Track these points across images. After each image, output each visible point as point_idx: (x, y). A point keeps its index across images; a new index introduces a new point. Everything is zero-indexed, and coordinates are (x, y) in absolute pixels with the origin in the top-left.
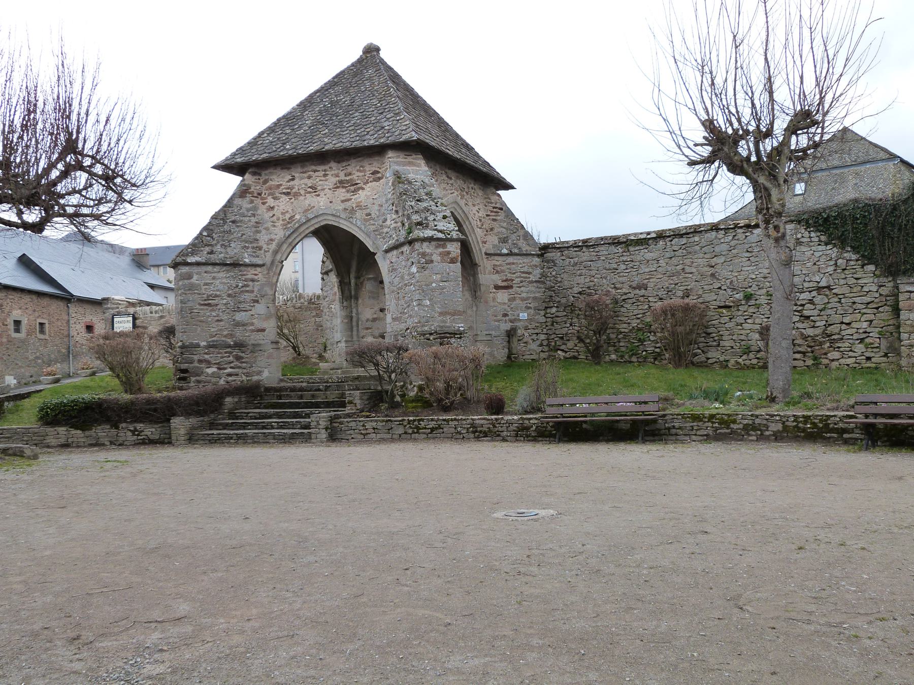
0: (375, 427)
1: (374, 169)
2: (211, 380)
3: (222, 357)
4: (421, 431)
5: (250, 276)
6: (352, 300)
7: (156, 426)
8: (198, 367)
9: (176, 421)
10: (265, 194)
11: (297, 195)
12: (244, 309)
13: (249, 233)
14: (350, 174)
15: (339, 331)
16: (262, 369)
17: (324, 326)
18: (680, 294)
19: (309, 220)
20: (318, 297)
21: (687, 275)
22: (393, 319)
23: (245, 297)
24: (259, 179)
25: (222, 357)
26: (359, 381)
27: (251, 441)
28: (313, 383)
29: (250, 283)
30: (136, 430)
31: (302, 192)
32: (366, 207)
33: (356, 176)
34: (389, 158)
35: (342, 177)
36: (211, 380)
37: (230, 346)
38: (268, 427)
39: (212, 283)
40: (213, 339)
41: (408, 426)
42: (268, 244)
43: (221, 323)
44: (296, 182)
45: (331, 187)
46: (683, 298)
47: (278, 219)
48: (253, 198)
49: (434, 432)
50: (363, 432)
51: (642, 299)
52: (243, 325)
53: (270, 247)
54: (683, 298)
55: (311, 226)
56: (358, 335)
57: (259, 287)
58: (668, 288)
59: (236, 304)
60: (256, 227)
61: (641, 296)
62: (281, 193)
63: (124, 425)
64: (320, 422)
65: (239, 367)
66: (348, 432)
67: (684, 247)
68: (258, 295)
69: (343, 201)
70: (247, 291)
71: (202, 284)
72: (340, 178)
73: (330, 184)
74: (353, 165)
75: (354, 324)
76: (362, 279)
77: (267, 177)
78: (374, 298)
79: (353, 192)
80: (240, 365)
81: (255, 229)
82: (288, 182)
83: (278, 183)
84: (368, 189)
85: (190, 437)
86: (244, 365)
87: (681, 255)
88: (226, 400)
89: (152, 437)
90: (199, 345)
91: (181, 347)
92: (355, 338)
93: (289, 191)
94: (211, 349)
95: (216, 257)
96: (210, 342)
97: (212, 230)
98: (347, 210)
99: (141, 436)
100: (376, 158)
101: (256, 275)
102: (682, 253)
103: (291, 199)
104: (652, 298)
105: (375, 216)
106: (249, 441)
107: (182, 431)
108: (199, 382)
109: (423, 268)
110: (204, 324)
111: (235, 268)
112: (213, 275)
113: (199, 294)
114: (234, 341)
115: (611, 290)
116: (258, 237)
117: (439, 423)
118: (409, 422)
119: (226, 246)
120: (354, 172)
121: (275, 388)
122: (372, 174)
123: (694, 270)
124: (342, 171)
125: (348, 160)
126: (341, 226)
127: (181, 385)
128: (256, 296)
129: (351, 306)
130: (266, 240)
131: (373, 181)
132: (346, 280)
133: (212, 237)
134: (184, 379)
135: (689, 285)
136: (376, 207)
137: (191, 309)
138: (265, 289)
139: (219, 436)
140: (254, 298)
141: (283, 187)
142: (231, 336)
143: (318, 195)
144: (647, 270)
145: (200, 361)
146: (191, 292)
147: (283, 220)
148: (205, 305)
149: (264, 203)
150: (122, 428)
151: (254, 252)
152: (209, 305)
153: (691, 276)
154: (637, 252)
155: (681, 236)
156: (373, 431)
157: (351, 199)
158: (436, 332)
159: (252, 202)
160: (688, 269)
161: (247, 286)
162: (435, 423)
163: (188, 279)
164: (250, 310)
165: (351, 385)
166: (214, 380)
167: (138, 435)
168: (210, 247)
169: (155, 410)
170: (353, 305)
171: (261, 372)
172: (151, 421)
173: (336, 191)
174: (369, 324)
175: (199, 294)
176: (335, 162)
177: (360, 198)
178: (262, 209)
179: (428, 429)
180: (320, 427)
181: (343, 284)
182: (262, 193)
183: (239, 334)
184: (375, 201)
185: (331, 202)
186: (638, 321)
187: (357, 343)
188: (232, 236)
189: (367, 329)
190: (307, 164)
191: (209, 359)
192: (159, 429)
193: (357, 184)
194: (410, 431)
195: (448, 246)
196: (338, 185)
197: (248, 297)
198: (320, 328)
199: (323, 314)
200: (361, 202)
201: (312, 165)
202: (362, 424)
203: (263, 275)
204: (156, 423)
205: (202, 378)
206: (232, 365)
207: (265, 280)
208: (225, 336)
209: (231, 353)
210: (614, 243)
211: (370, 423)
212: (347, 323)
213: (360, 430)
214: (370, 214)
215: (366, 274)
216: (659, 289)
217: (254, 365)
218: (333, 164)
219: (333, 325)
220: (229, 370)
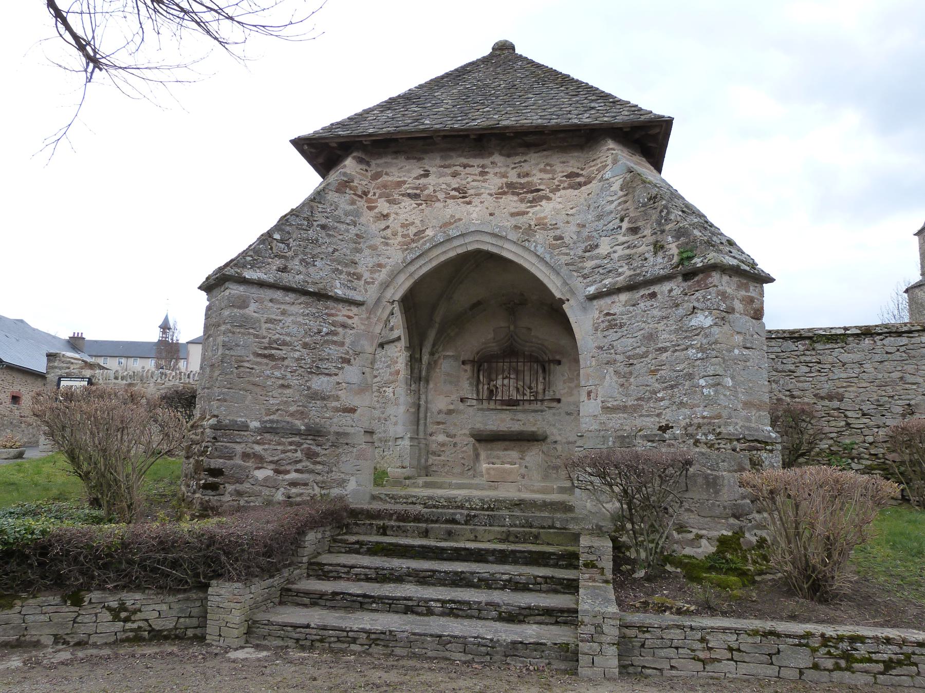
0: (735, 646)
1: (570, 170)
2: (261, 492)
3: (284, 452)
4: (856, 666)
5: (340, 319)
7: (171, 599)
8: (240, 466)
9: (222, 592)
10: (375, 194)
11: (430, 200)
12: (327, 371)
13: (345, 249)
14: (527, 175)
16: (347, 477)
18: (900, 410)
19: (449, 240)
21: (907, 386)
22: (603, 408)
23: (330, 352)
24: (367, 171)
25: (284, 452)
26: (522, 510)
27: (404, 652)
28: (434, 506)
29: (340, 330)
30: (123, 607)
31: (441, 196)
32: (555, 227)
33: (537, 178)
34: (608, 149)
35: (513, 177)
36: (261, 492)
37: (298, 433)
38: (420, 610)
39: (280, 321)
40: (272, 417)
41: (824, 650)
42: (372, 271)
43: (287, 391)
44: (431, 180)
45: (493, 191)
46: (904, 416)
47: (395, 234)
48: (356, 198)
49: (894, 672)
50: (701, 655)
51: (836, 413)
52: (323, 399)
53: (376, 276)
54: (904, 416)
55: (452, 249)
56: (425, 431)
57: (352, 339)
58: (878, 401)
59: (314, 362)
60: (355, 243)
61: (834, 409)
62: (403, 195)
63: (95, 596)
64: (606, 629)
65: (312, 472)
66: (662, 653)
67: (902, 349)
68: (351, 352)
69: (513, 215)
70: (335, 343)
71: (263, 320)
72: (509, 180)
73: (493, 187)
74: (533, 162)
75: (422, 415)
76: (437, 356)
77: (379, 170)
78: (451, 383)
79: (530, 202)
80: (311, 466)
81: (354, 245)
82: (417, 178)
83: (399, 180)
84: (559, 200)
85: (249, 627)
86: (319, 467)
87: (898, 358)
88: (307, 538)
89: (158, 625)
90: (248, 426)
91: (214, 428)
92: (421, 435)
93: (418, 192)
94: (267, 436)
95: (291, 278)
96: (266, 422)
97: (289, 233)
98: (520, 228)
99: (134, 622)
100: (576, 154)
101: (350, 317)
102: (901, 357)
103: (421, 204)
104: (853, 412)
105: (571, 241)
106: (398, 651)
107: (236, 617)
108: (239, 494)
109: (723, 319)
110: (258, 390)
111: (319, 301)
112: (283, 307)
113: (257, 336)
114: (306, 425)
115: (784, 398)
116: (357, 259)
117: (908, 649)
118: (824, 638)
119: (307, 263)
120: (534, 172)
121: (368, 511)
122: (566, 176)
123: (920, 380)
124: (513, 168)
125: (524, 154)
126: (505, 254)
127: (207, 498)
128: (347, 353)
130: (370, 265)
131: (568, 188)
132: (417, 356)
133: (288, 245)
134: (213, 487)
135: (913, 399)
136: (574, 228)
137: (240, 361)
138: (362, 342)
139: (325, 633)
140: (343, 356)
141: (408, 186)
142: (302, 414)
143: (469, 203)
144: (844, 375)
145: (246, 456)
146: (242, 330)
147: (404, 236)
148: (265, 356)
149: (370, 208)
150: (90, 602)
151: (349, 281)
152: (271, 357)
153: (914, 387)
154: (828, 352)
155: (899, 334)
156: (729, 656)
157: (528, 213)
158: (744, 438)
159: (353, 203)
160: (910, 379)
161: (335, 333)
162: (896, 649)
163: (240, 307)
164: (336, 375)
165: (517, 517)
166: (266, 492)
167: (126, 620)
168: (283, 261)
169: (175, 564)
170: (422, 390)
171: (344, 481)
172: (161, 588)
173: (501, 198)
174: (441, 418)
175: (257, 336)
176: (501, 154)
177: (543, 211)
178: (367, 217)
179: (877, 662)
180: (603, 638)
181: (414, 360)
182: (369, 192)
183: (316, 414)
184: (570, 219)
185: (491, 215)
186: (831, 442)
188: (319, 250)
189: (439, 423)
190: (452, 154)
191: (262, 453)
192: (176, 606)
193: (538, 190)
194: (829, 663)
195: (751, 288)
196: (506, 190)
197: (334, 351)
200: (545, 218)
201: (460, 156)
202: (698, 635)
203: (361, 319)
204: (173, 591)
205: (246, 486)
206: (299, 466)
207: (363, 327)
208: (292, 415)
209: (299, 444)
210: (791, 338)
211: (720, 636)
213: (693, 651)
214: (560, 238)
216: (863, 401)
217: (334, 469)
218: (497, 158)
219: (387, 414)
220: (293, 476)
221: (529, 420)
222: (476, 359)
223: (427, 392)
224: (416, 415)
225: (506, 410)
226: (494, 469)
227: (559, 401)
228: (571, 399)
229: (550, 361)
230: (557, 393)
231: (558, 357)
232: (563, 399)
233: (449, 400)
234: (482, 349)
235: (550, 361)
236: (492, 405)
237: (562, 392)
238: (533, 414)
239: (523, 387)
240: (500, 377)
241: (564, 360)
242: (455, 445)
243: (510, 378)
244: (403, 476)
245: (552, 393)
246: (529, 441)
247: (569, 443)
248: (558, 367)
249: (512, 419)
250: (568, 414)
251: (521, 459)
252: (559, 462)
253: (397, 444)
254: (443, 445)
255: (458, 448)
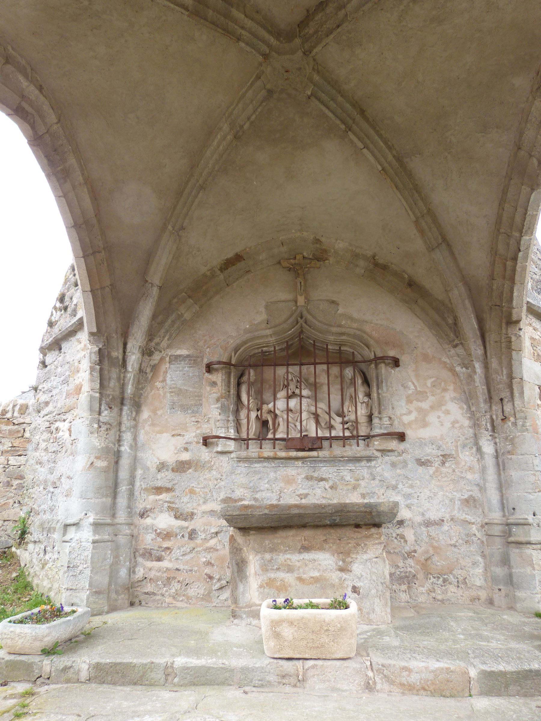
6: (125, 408)
15: (76, 492)
17: (29, 477)
20: (24, 409)
75: (123, 474)
76: (157, 357)
78: (184, 408)
92: (122, 517)
129: (120, 424)
132: (117, 354)
170: (126, 422)
187: (126, 530)
189: (159, 490)
198: (15, 483)
199: (30, 447)
212: (105, 470)
215: (169, 347)
219: (57, 474)
221: (342, 478)
222: (233, 362)
223: (135, 427)
224: (111, 475)
225: (297, 459)
226: (291, 623)
227: (401, 437)
228: (425, 433)
229: (378, 360)
230: (396, 423)
231: (392, 353)
232: (409, 433)
233: (180, 442)
234: (245, 343)
235: (378, 360)
236: (268, 451)
237: (406, 419)
238: (351, 466)
239: (329, 414)
240: (281, 394)
241: (404, 359)
242: (192, 534)
243: (301, 396)
244: (38, 646)
245: (386, 421)
246: (357, 526)
247: (428, 524)
248: (395, 372)
249: (309, 478)
250: (421, 463)
251: (342, 570)
252: (411, 566)
253: (67, 538)
254: (167, 535)
255: (199, 541)
